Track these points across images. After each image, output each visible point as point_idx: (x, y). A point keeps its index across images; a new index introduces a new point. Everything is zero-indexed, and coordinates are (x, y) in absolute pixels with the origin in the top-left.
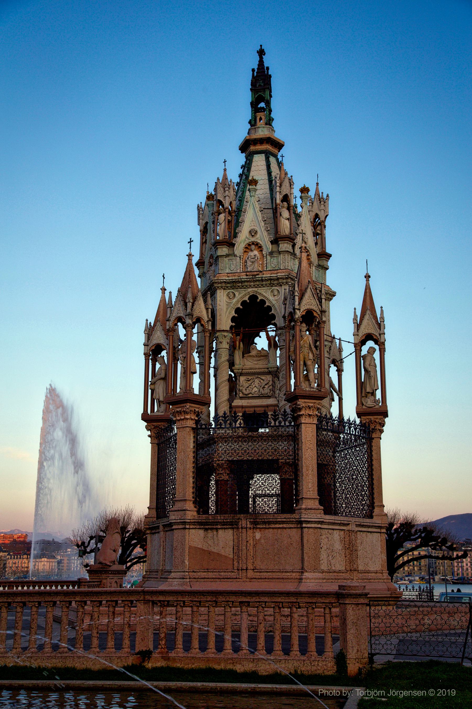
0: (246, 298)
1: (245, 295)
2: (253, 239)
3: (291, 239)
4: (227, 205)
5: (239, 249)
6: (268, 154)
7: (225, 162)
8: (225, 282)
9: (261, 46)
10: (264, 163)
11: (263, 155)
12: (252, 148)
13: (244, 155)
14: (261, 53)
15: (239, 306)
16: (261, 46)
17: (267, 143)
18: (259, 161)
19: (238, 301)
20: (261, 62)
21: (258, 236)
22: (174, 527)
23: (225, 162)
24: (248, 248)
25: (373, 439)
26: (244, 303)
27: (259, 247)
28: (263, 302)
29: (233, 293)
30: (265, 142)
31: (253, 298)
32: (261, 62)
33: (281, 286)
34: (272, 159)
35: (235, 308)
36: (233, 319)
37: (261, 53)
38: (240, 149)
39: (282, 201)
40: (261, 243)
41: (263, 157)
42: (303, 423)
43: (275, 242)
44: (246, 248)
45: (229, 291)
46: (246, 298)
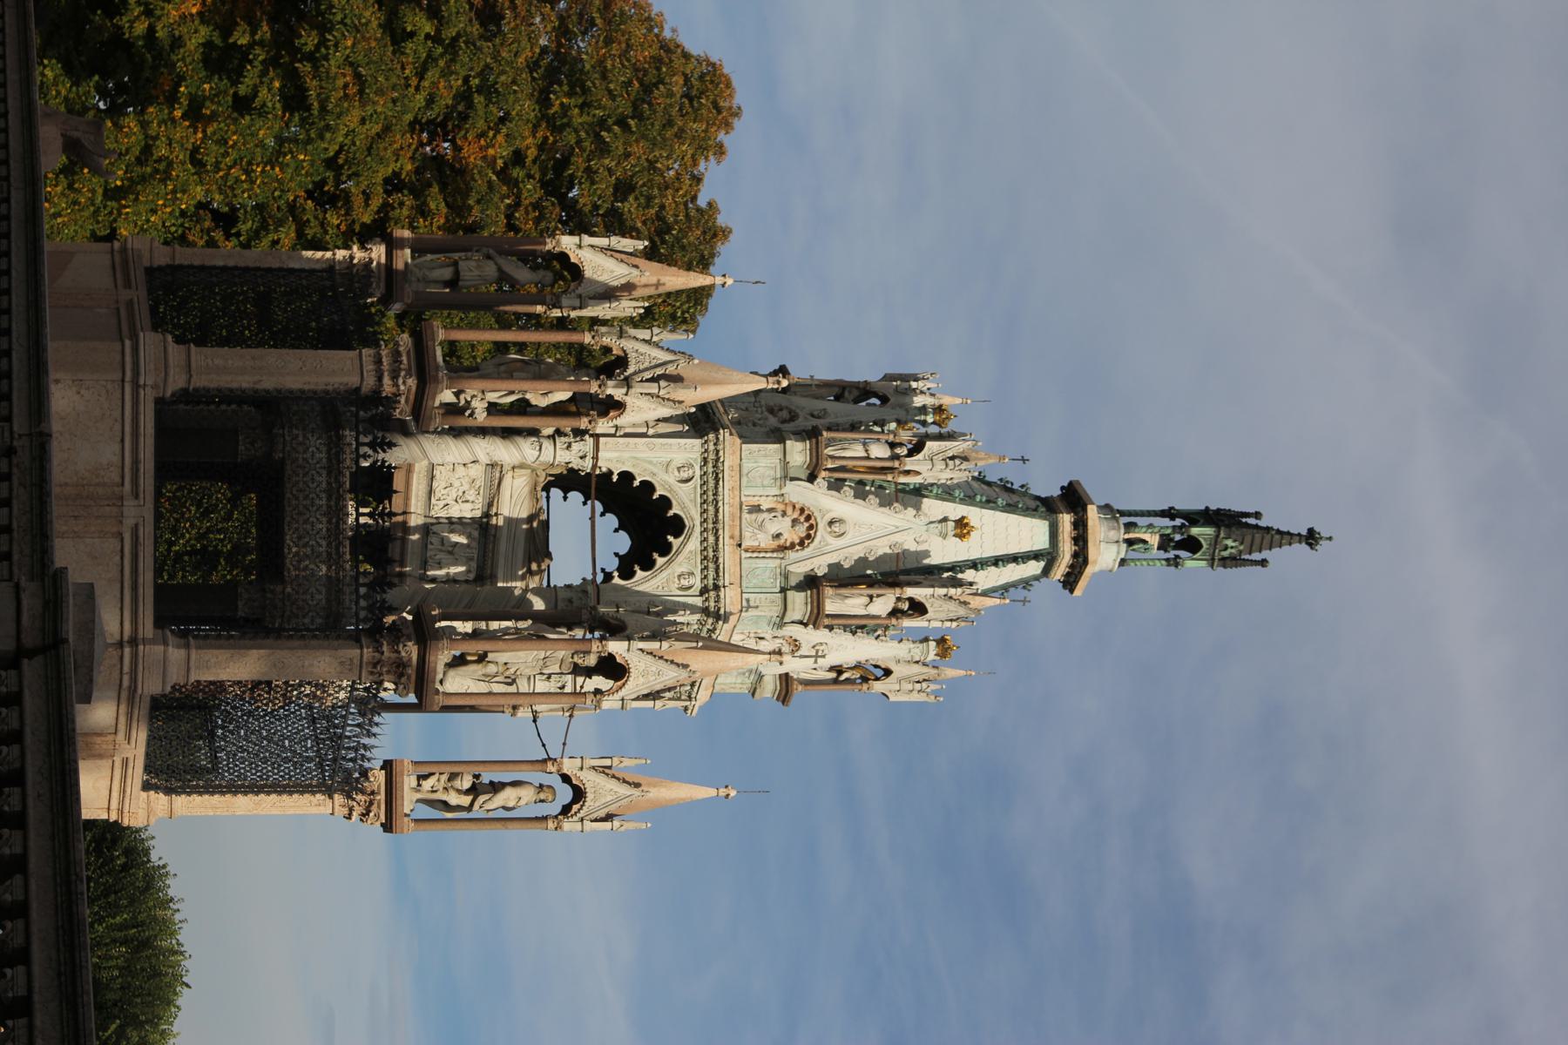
2: (822, 525)
3: (816, 618)
4: (910, 464)
5: (800, 492)
6: (1048, 557)
7: (1024, 460)
8: (717, 460)
9: (1330, 539)
10: (1025, 547)
11: (1046, 545)
12: (1066, 520)
13: (1057, 492)
14: (1311, 538)
16: (1330, 539)
17: (1075, 555)
18: (1031, 533)
20: (1285, 537)
21: (830, 539)
22: (128, 343)
23: (1024, 460)
24: (806, 516)
25: (331, 797)
28: (665, 550)
31: (677, 526)
32: (1285, 537)
34: (1035, 567)
36: (627, 476)
37: (1311, 538)
38: (1071, 483)
39: (911, 600)
41: (1041, 541)
43: (811, 583)
44: (802, 510)
45: (697, 468)
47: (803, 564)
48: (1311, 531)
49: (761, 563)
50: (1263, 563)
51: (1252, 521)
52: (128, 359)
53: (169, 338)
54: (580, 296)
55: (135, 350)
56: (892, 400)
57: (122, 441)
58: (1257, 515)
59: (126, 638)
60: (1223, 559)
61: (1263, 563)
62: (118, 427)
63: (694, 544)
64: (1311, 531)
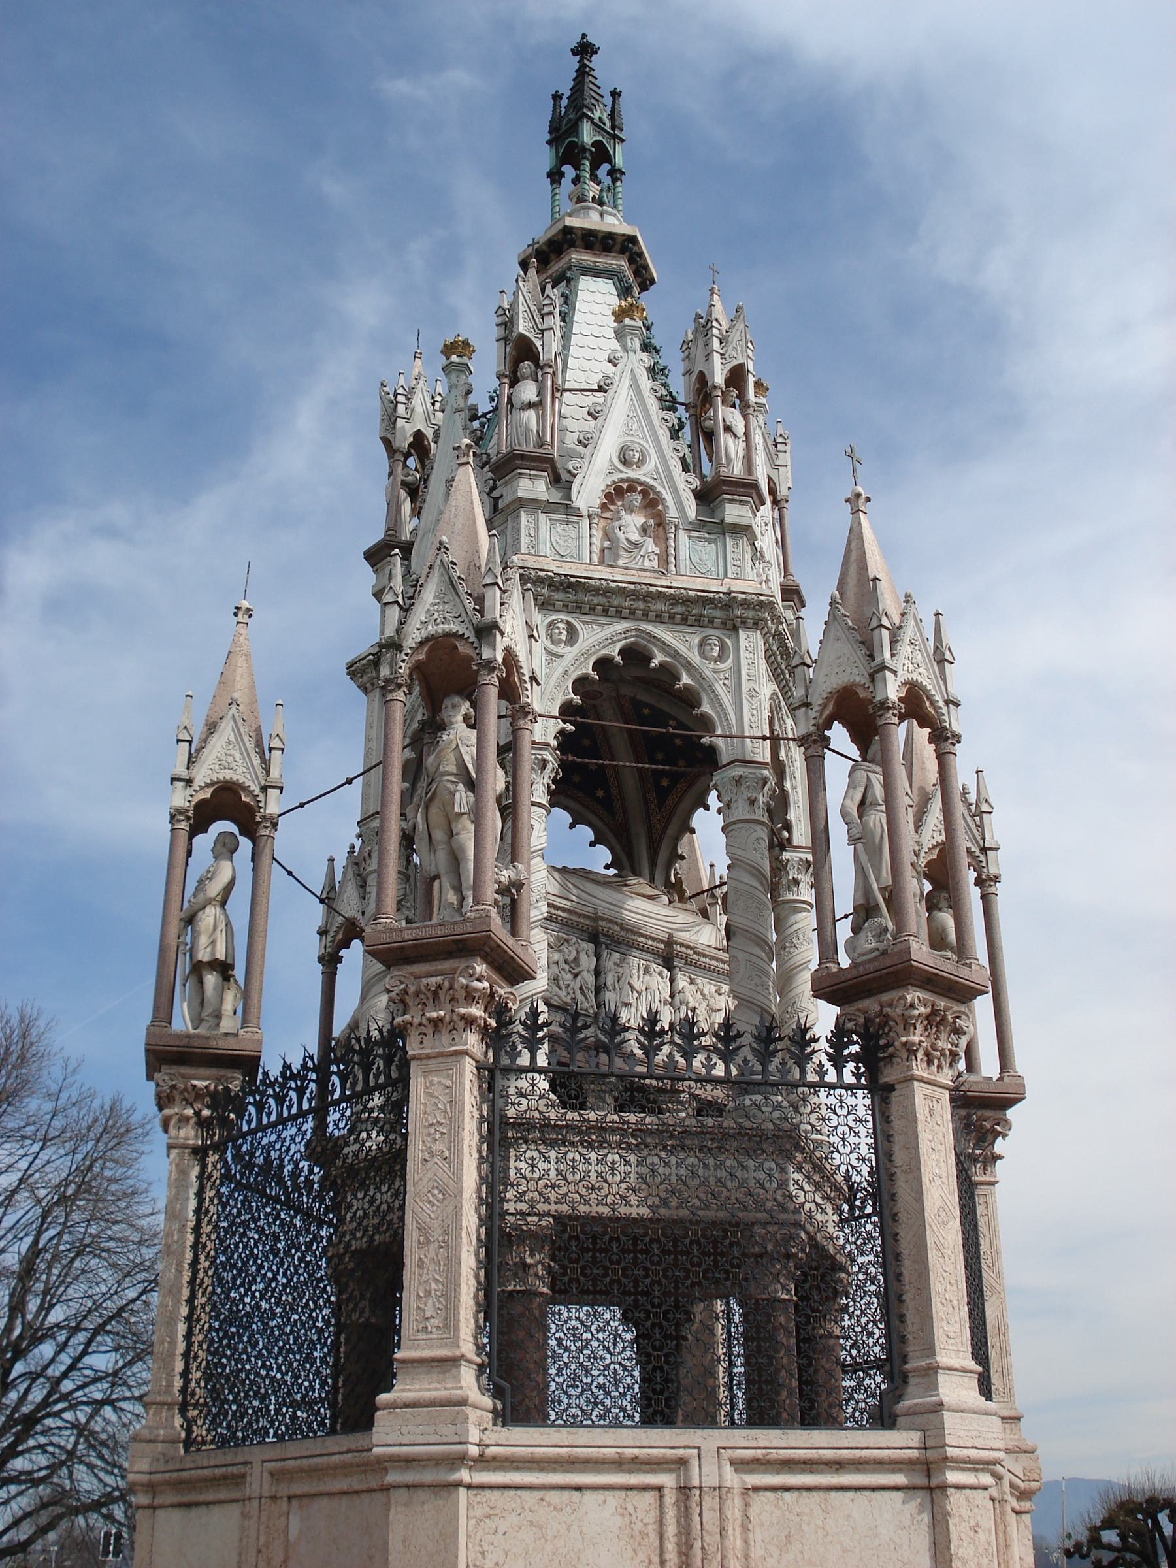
0: (614, 651)
1: (612, 641)
2: (631, 474)
15: (588, 669)
19: (587, 654)
20: (583, 73)
21: (649, 466)
22: (392, 1478)
24: (616, 494)
26: (603, 664)
27: (651, 502)
29: (568, 622)
30: (618, 247)
31: (635, 655)
32: (583, 73)
33: (735, 629)
35: (574, 676)
40: (659, 488)
42: (922, 1080)
43: (707, 496)
46: (614, 651)
47: (681, 499)
48: (574, 52)
49: (684, 553)
50: (615, 94)
51: (564, 102)
52: (428, 1477)
53: (383, 1397)
54: (264, 789)
55: (408, 1462)
56: (420, 426)
57: (578, 1488)
58: (557, 97)
59: (920, 1480)
60: (613, 127)
61: (615, 94)
62: (553, 1496)
63: (663, 633)
64: (574, 52)
